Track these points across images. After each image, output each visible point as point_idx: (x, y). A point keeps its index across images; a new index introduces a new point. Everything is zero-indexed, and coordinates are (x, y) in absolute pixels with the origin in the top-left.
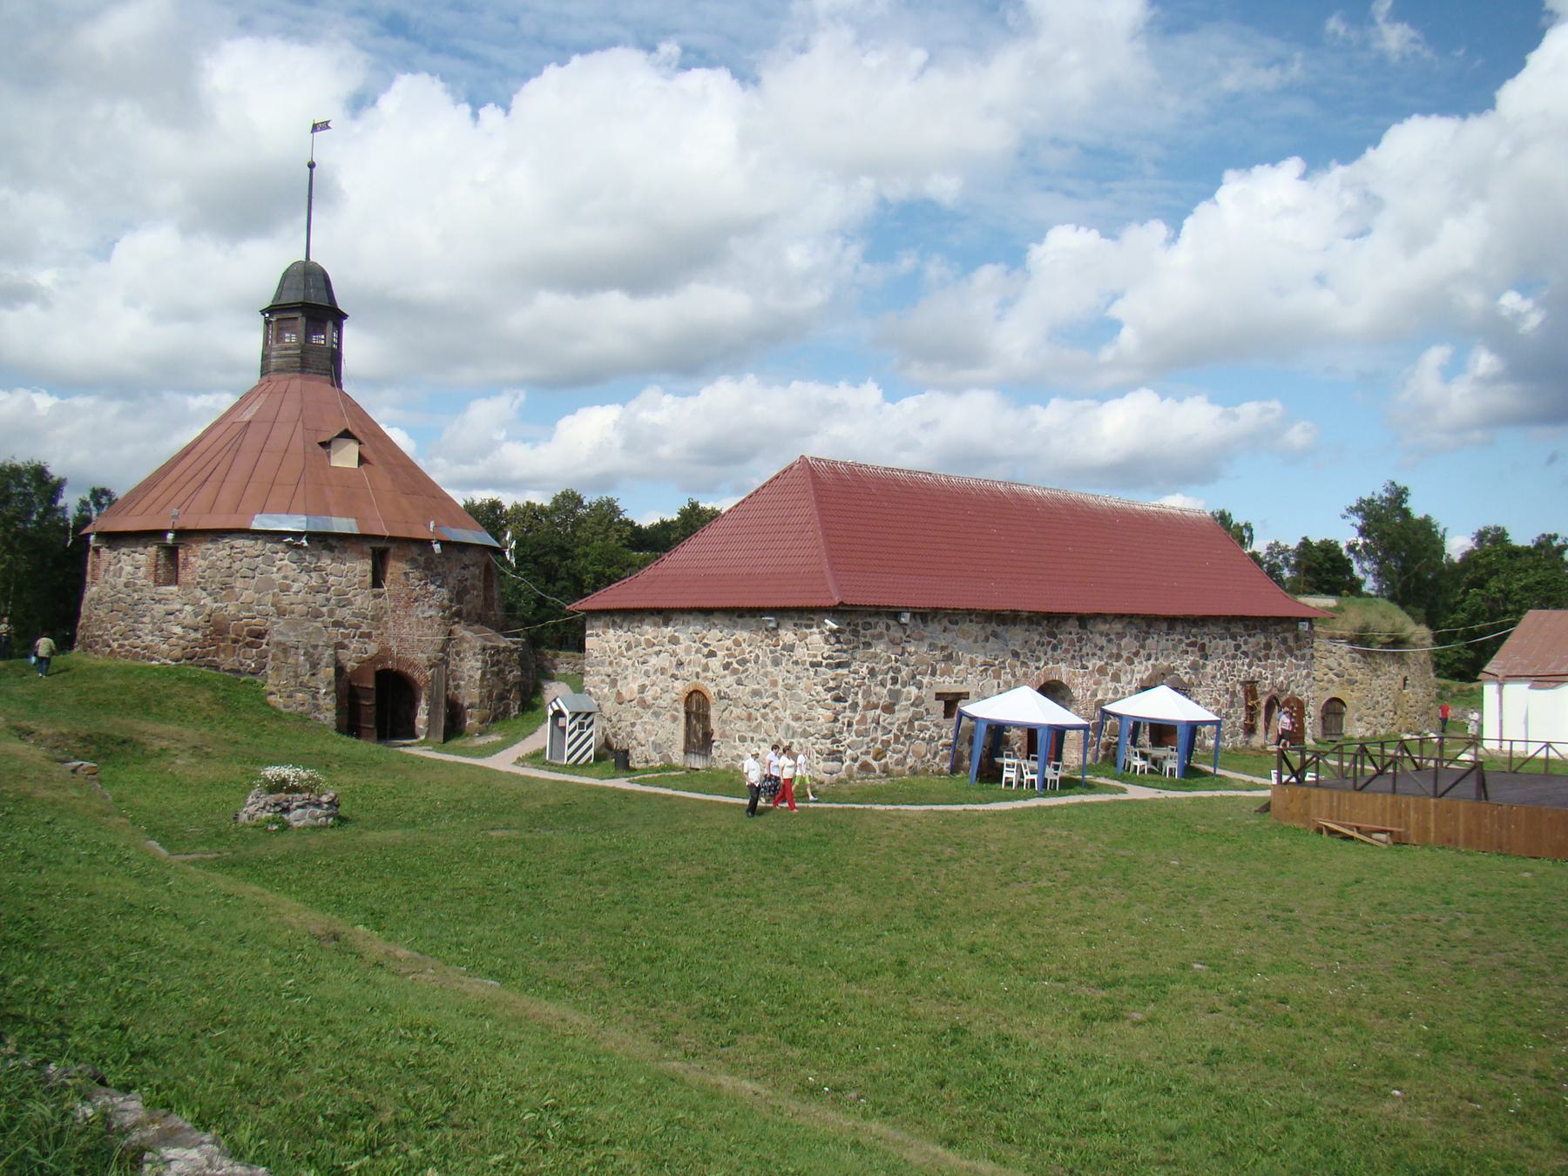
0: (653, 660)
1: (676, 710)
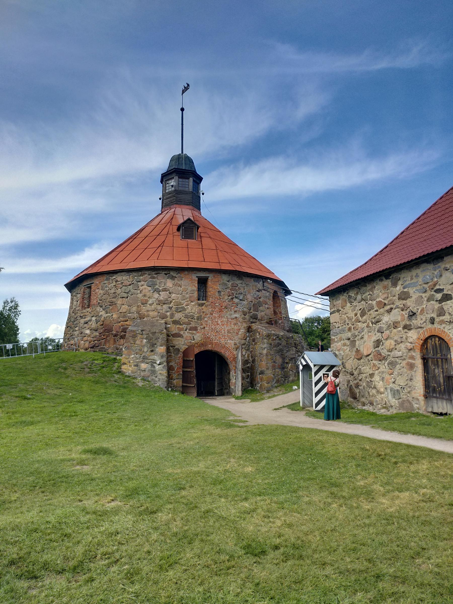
0: (386, 319)
1: (412, 358)
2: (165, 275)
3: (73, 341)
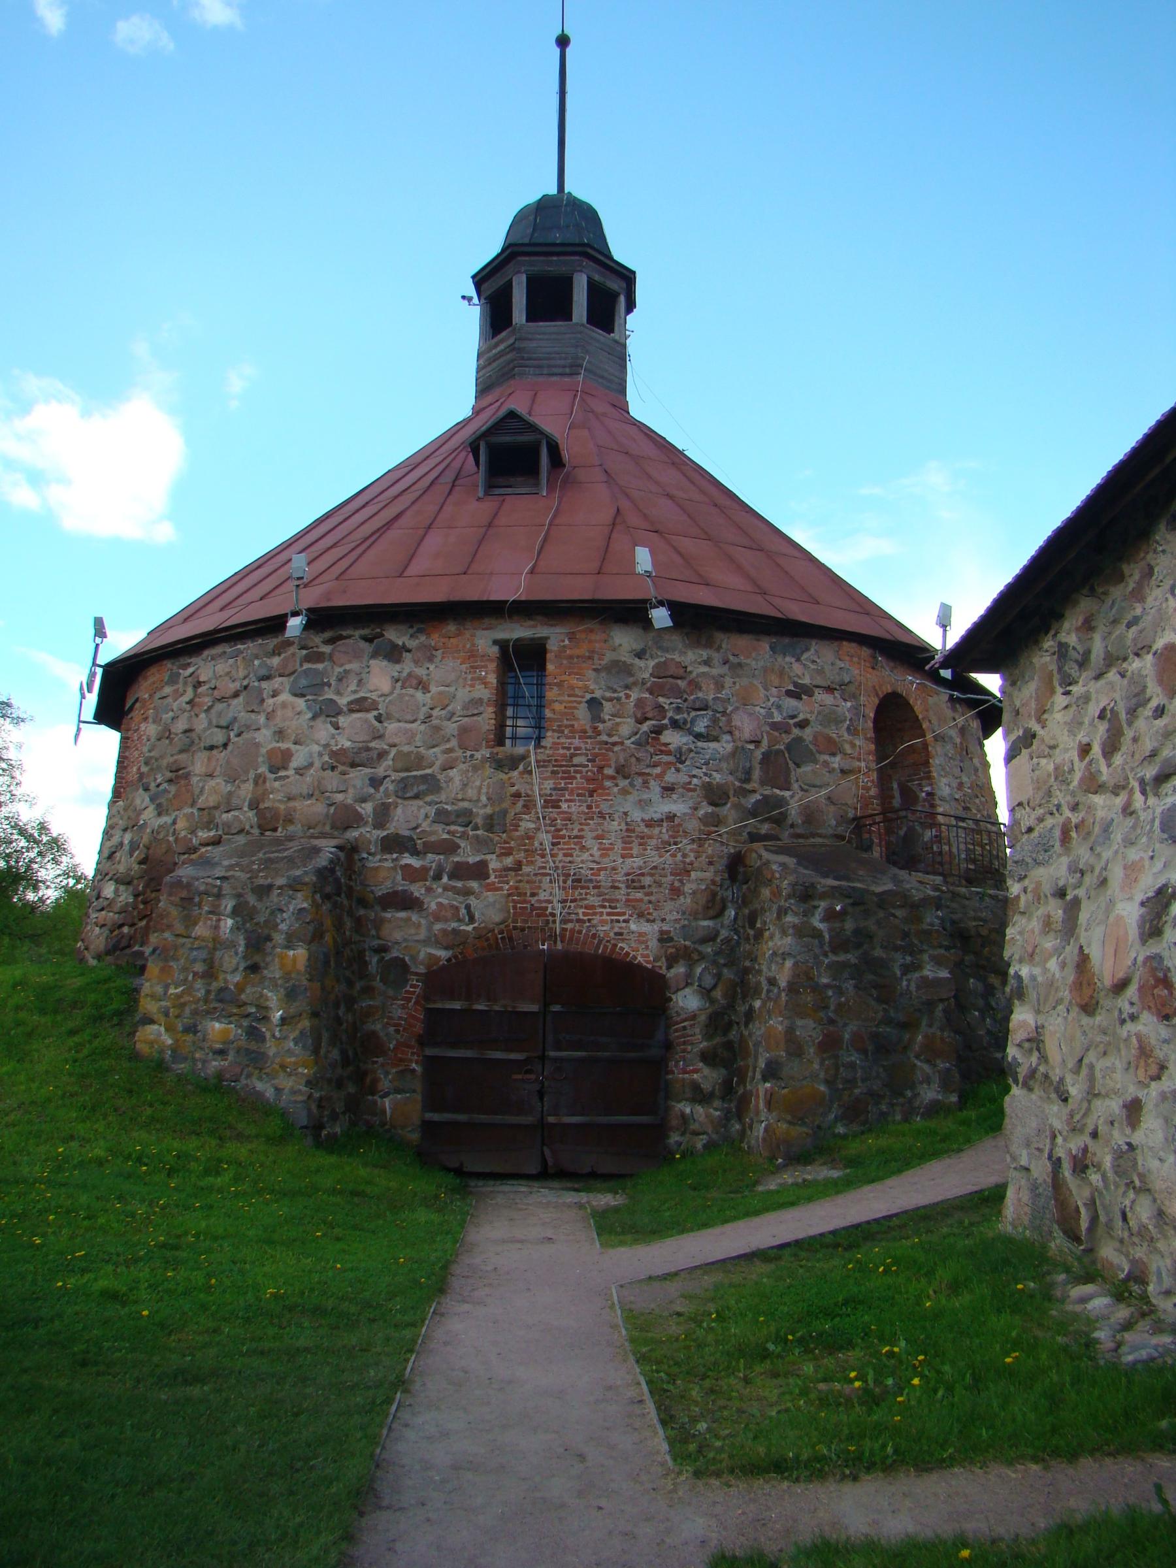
2: (363, 645)
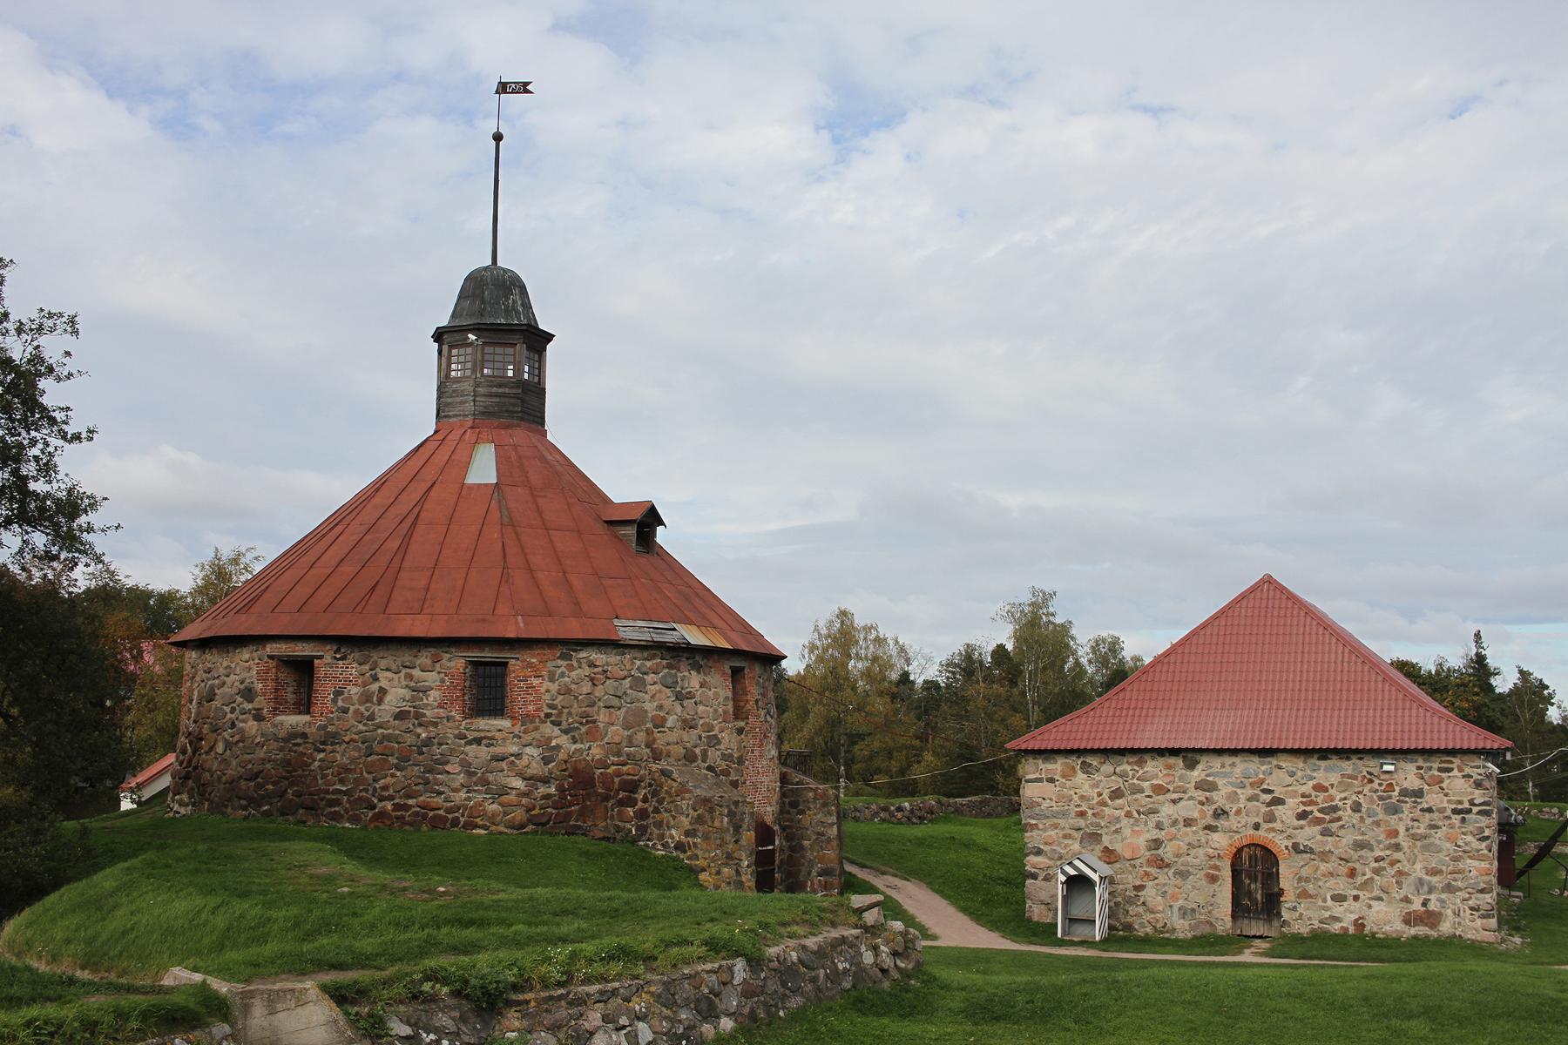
0: (1167, 810)
1: (1217, 868)
3: (439, 800)
